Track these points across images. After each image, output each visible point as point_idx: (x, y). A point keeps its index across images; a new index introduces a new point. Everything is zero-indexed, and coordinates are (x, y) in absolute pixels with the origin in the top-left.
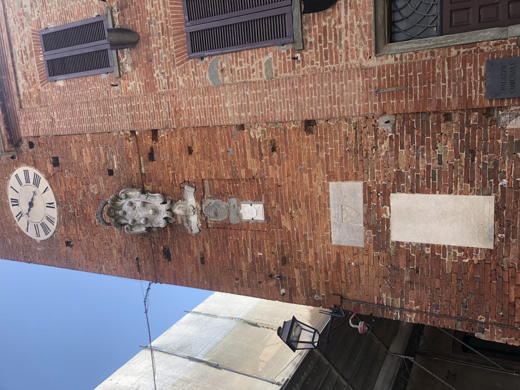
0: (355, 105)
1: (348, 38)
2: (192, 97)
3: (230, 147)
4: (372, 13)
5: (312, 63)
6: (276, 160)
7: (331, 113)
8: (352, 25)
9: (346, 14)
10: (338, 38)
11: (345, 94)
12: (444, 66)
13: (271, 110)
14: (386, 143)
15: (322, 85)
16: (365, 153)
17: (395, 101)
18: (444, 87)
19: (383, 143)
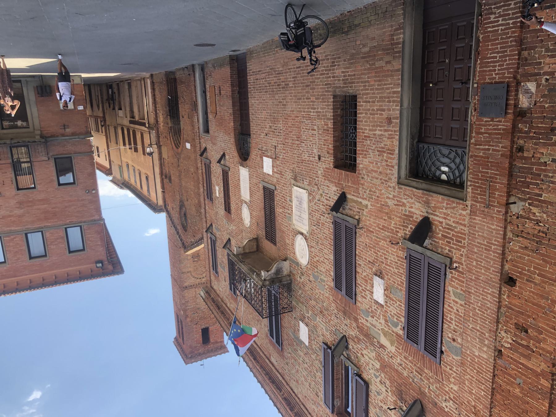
0: (494, 229)
1: (452, 220)
2: (465, 384)
3: (515, 379)
4: (441, 196)
5: (462, 255)
6: (535, 334)
7: (497, 253)
8: (445, 214)
9: (437, 216)
11: (485, 235)
12: (479, 149)
13: (487, 311)
14: (534, 210)
15: (476, 253)
16: (541, 234)
17: (497, 193)
18: (493, 150)
19: (535, 213)
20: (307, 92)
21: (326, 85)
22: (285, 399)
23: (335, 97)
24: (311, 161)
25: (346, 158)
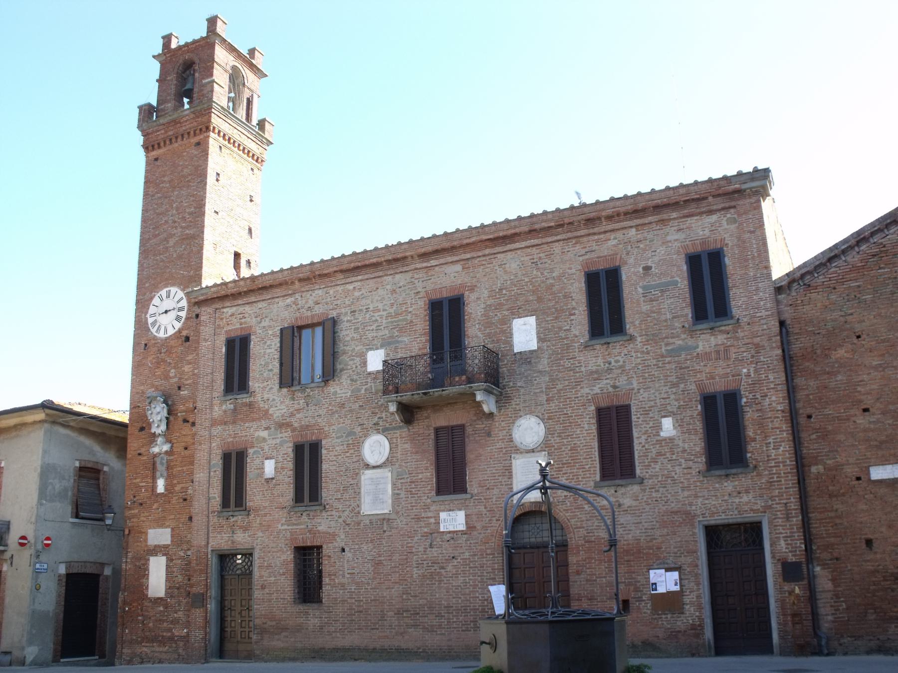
10: (219, 533)
22: (405, 258)
23: (321, 602)
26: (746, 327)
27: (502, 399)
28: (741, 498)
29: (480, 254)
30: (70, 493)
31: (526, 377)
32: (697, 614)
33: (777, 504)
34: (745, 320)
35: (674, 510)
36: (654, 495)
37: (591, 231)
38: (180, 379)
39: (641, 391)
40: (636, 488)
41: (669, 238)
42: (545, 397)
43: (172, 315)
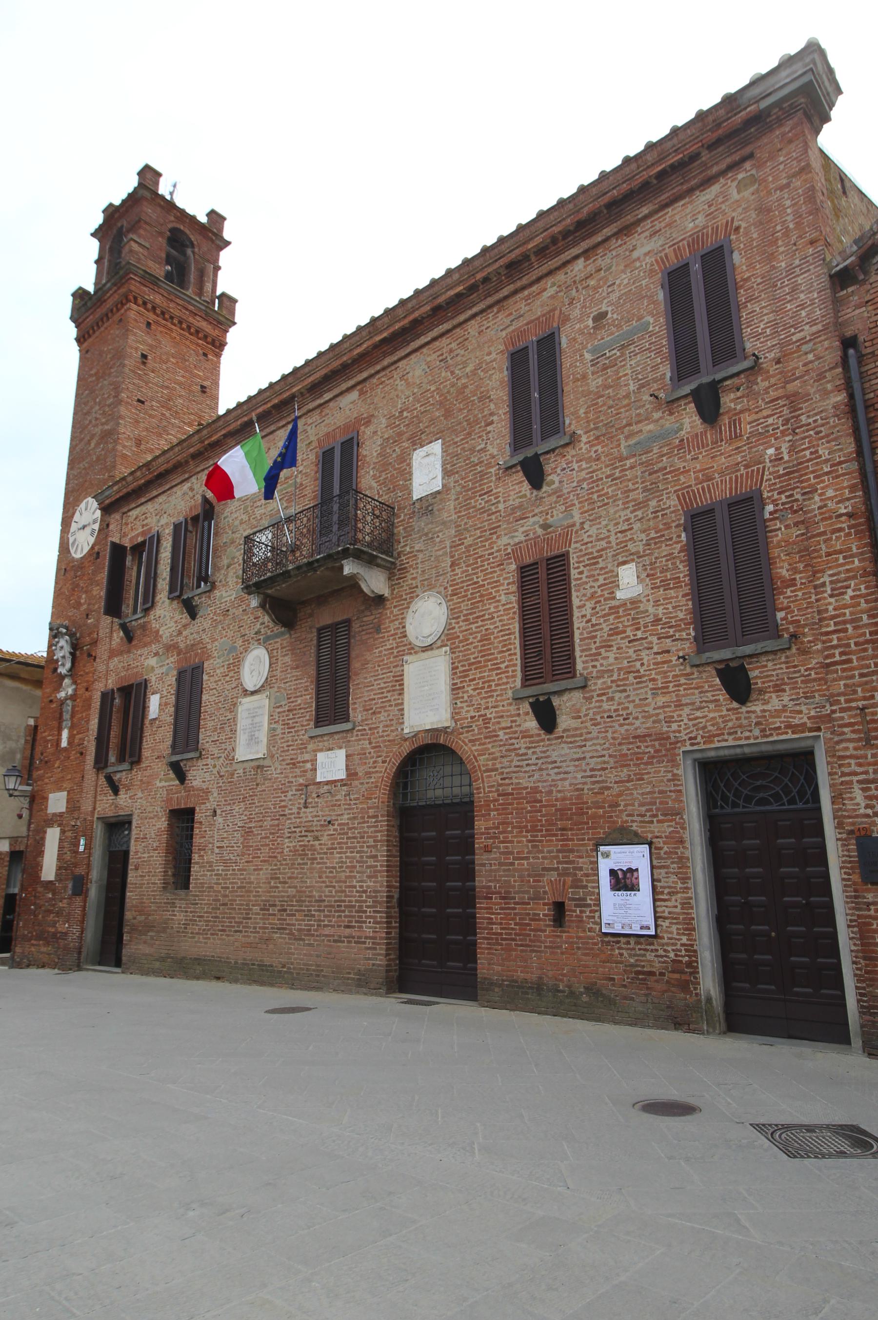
20: (225, 896)
21: (197, 904)
24: (229, 804)
25: (183, 820)
26: (773, 369)
27: (394, 571)
28: (766, 702)
29: (378, 367)
30: (18, 756)
31: (426, 534)
32: (684, 940)
33: (842, 710)
34: (771, 356)
35: (639, 732)
36: (605, 706)
37: (519, 284)
38: (89, 604)
39: (586, 526)
40: (577, 695)
41: (635, 254)
42: (449, 561)
43: (88, 530)
